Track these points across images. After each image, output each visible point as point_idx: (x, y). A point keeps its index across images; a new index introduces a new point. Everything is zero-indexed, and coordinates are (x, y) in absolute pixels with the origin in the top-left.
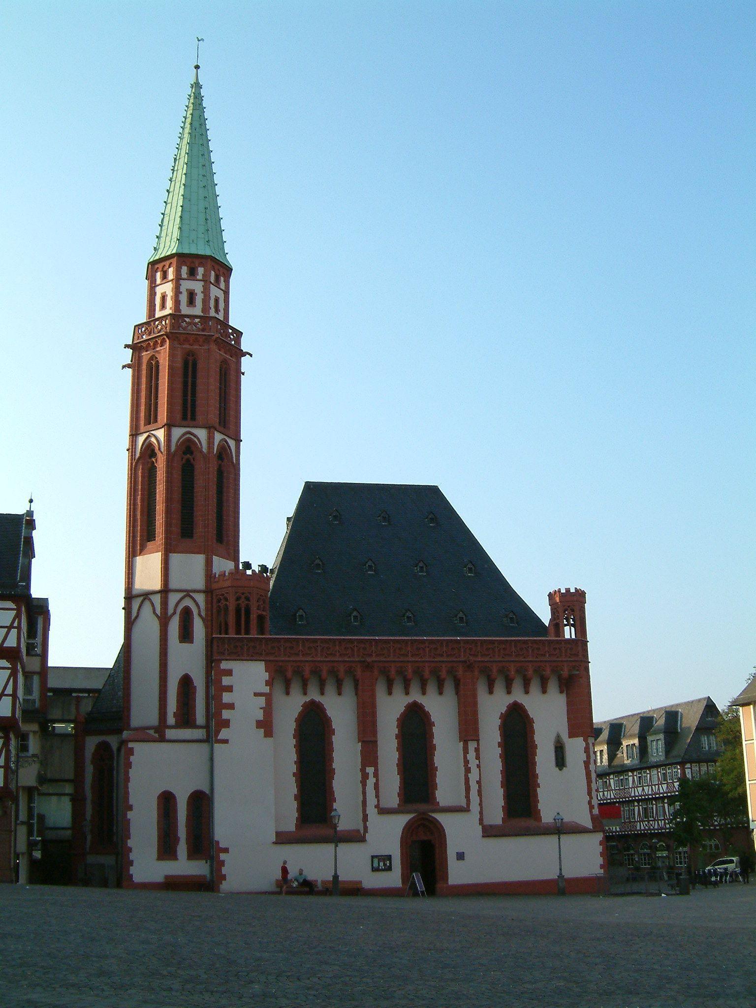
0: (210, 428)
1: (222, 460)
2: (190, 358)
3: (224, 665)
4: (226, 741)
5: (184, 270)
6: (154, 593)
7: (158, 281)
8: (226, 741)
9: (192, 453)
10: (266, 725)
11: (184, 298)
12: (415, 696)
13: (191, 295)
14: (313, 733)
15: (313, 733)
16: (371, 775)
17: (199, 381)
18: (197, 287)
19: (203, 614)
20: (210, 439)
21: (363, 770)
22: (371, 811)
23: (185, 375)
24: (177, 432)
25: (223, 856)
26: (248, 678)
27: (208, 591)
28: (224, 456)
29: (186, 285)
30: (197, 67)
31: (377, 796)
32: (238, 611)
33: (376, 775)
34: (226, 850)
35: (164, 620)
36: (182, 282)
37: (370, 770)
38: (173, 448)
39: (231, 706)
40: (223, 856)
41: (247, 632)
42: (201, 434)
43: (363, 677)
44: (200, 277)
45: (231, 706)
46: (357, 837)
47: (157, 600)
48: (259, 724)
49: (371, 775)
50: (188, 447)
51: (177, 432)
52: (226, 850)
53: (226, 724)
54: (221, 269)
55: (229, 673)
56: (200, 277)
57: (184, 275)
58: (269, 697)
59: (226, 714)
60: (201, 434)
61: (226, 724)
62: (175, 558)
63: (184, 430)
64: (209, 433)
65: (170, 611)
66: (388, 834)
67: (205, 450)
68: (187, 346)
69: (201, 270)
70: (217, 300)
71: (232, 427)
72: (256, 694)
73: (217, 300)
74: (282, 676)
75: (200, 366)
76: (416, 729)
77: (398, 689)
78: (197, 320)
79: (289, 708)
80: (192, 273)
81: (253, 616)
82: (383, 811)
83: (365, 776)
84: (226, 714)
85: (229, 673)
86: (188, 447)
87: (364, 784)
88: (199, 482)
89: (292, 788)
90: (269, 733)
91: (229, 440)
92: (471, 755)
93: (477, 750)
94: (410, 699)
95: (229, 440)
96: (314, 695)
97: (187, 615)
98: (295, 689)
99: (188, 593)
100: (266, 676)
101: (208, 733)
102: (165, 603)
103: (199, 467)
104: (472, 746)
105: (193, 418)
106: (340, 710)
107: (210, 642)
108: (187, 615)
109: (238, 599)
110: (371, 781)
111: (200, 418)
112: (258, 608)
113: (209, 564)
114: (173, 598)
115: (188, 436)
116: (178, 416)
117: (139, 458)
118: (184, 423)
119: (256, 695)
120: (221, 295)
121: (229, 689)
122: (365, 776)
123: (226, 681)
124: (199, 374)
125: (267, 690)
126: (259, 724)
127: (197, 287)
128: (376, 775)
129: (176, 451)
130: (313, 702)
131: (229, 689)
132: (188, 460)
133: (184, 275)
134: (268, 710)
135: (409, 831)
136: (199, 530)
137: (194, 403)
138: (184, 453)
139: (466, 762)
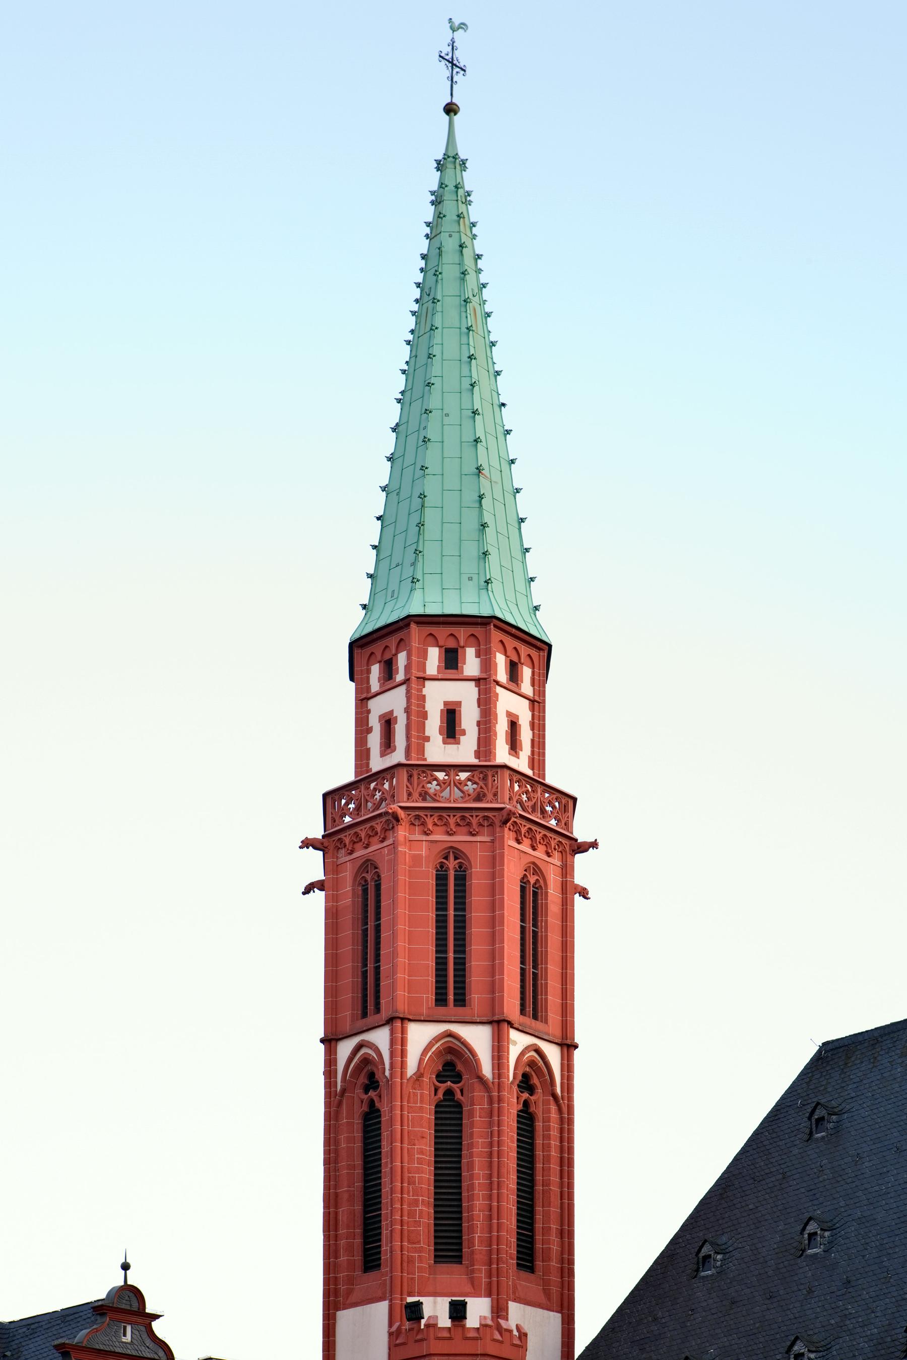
1: (458, 1078)
28: (460, 1067)
36: (372, 704)
44: (400, 677)
54: (462, 633)
57: (375, 686)
68: (360, 853)
69: (402, 659)
70: (451, 715)
71: (476, 996)
73: (451, 715)
105: (378, 1010)
115: (363, 1051)
118: (361, 1024)
120: (465, 694)
127: (394, 701)
129: (344, 1091)
132: (372, 1103)
133: (375, 686)
137: (377, 970)
138: (366, 1089)
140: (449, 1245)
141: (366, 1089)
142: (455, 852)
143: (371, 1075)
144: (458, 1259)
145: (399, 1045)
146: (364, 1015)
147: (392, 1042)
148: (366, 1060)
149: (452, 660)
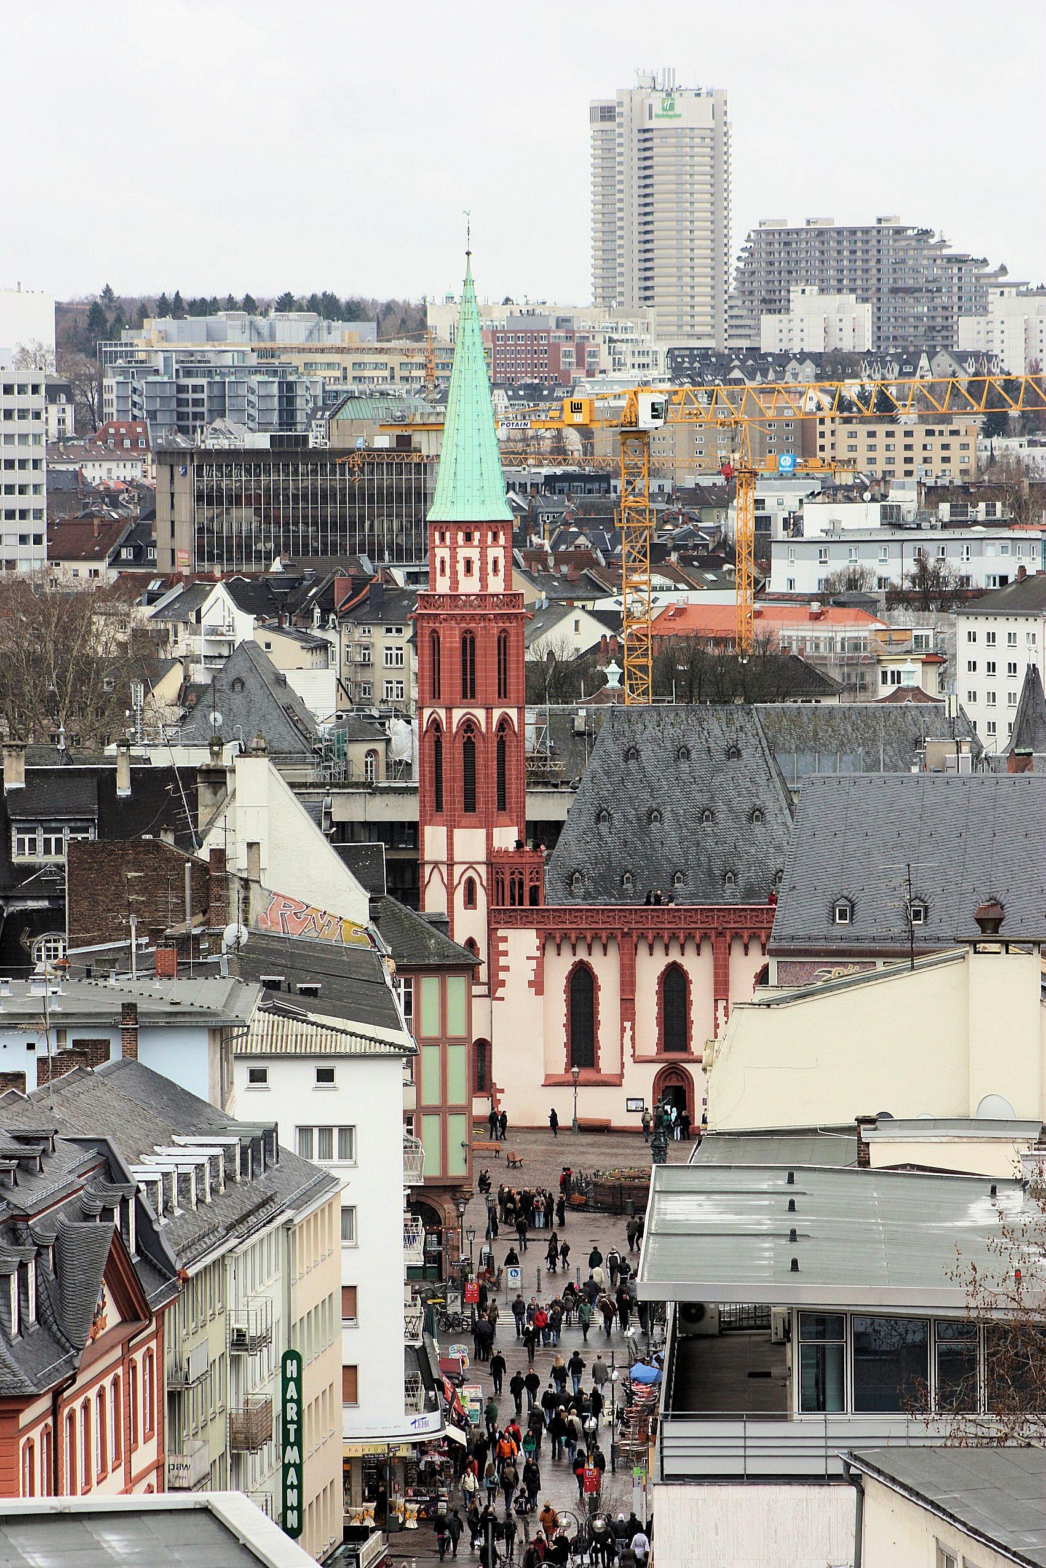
0: (489, 710)
2: (468, 636)
3: (500, 933)
4: (502, 999)
5: (461, 536)
6: (442, 863)
7: (437, 542)
8: (502, 999)
9: (472, 731)
10: (538, 985)
11: (461, 567)
12: (675, 956)
13: (468, 564)
14: (582, 988)
15: (582, 988)
16: (628, 1029)
17: (478, 659)
18: (474, 554)
19: (485, 883)
20: (489, 718)
21: (622, 1024)
22: (628, 1060)
23: (464, 654)
24: (458, 714)
25: (499, 1096)
26: (521, 943)
27: (489, 864)
29: (463, 553)
30: (468, 253)
31: (633, 1047)
32: (513, 882)
33: (632, 1028)
34: (502, 1091)
35: (450, 890)
37: (628, 1025)
38: (454, 730)
39: (506, 969)
40: (499, 1096)
41: (521, 904)
42: (480, 714)
43: (627, 941)
44: (476, 543)
45: (506, 969)
46: (615, 1082)
47: (444, 869)
48: (531, 984)
49: (628, 1029)
50: (469, 725)
51: (458, 714)
52: (502, 1091)
53: (502, 983)
54: (499, 525)
55: (505, 939)
56: (476, 543)
58: (540, 962)
59: (502, 975)
60: (480, 714)
61: (502, 983)
62: (458, 833)
63: (465, 711)
64: (487, 713)
65: (456, 882)
66: (641, 1082)
67: (484, 730)
69: (477, 535)
70: (495, 562)
72: (528, 958)
73: (495, 562)
74: (550, 939)
75: (478, 644)
76: (674, 985)
77: (659, 951)
78: (473, 598)
79: (559, 968)
80: (468, 538)
81: (526, 889)
82: (638, 1060)
83: (623, 1030)
84: (502, 975)
85: (505, 939)
86: (469, 725)
87: (622, 1037)
88: (480, 761)
89: (562, 1036)
90: (540, 992)
91: (508, 711)
92: (721, 1012)
93: (726, 1008)
94: (670, 959)
95: (508, 711)
96: (582, 955)
97: (470, 884)
98: (566, 951)
99: (471, 865)
100: (537, 942)
101: (489, 989)
102: (451, 874)
103: (480, 746)
104: (721, 1004)
105: (473, 696)
106: (606, 969)
107: (490, 912)
108: (470, 884)
109: (512, 874)
110: (628, 1034)
111: (478, 696)
112: (531, 880)
113: (489, 838)
114: (458, 870)
116: (459, 696)
117: (426, 731)
119: (528, 958)
121: (505, 953)
122: (623, 1030)
123: (502, 947)
124: (478, 652)
125: (538, 954)
126: (531, 984)
128: (632, 1028)
129: (457, 733)
130: (581, 962)
131: (505, 953)
134: (539, 972)
135: (661, 1076)
136: (480, 806)
137: (473, 681)
138: (466, 731)
139: (716, 1019)
140: (502, 805)
141: (466, 731)
142: (504, 630)
143: (469, 726)
144: (504, 809)
145: (489, 718)
146: (465, 696)
147: (487, 718)
148: (469, 720)
149: (495, 537)
